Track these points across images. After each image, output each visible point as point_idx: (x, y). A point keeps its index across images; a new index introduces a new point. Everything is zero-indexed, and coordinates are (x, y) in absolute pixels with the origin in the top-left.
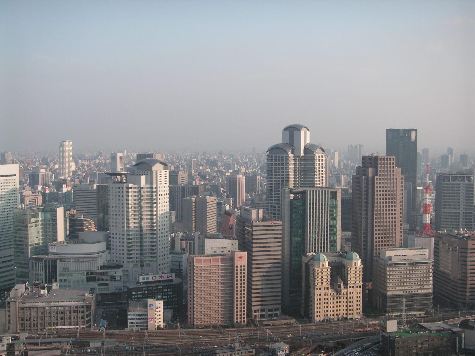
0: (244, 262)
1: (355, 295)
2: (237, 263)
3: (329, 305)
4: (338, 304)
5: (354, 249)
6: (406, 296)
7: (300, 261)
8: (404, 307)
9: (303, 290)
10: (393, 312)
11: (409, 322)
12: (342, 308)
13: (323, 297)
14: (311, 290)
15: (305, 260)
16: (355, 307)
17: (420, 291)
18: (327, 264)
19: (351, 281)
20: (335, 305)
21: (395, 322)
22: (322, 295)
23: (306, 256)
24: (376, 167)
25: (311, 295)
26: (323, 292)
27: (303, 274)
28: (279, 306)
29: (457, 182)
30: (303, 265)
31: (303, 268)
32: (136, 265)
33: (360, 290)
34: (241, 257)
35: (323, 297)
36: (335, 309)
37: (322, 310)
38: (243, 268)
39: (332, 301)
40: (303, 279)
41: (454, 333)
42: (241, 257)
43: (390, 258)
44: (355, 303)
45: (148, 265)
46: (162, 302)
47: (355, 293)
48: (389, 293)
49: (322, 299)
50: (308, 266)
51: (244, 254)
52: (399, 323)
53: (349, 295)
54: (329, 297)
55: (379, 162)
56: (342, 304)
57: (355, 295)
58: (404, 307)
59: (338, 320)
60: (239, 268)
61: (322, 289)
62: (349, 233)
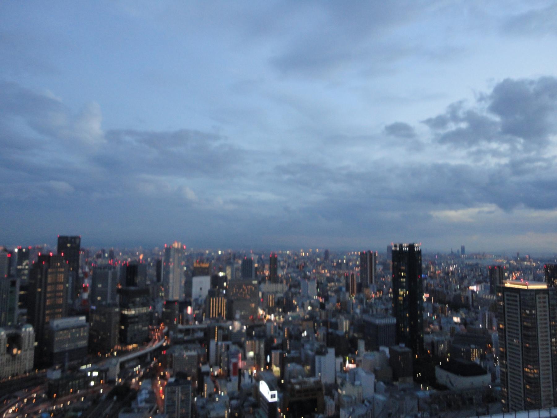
1: (28, 357)
18: (5, 337)
29: (106, 270)
33: (33, 352)
43: (57, 326)
52: (63, 372)
53: (23, 358)
57: (28, 357)
62: (25, 311)
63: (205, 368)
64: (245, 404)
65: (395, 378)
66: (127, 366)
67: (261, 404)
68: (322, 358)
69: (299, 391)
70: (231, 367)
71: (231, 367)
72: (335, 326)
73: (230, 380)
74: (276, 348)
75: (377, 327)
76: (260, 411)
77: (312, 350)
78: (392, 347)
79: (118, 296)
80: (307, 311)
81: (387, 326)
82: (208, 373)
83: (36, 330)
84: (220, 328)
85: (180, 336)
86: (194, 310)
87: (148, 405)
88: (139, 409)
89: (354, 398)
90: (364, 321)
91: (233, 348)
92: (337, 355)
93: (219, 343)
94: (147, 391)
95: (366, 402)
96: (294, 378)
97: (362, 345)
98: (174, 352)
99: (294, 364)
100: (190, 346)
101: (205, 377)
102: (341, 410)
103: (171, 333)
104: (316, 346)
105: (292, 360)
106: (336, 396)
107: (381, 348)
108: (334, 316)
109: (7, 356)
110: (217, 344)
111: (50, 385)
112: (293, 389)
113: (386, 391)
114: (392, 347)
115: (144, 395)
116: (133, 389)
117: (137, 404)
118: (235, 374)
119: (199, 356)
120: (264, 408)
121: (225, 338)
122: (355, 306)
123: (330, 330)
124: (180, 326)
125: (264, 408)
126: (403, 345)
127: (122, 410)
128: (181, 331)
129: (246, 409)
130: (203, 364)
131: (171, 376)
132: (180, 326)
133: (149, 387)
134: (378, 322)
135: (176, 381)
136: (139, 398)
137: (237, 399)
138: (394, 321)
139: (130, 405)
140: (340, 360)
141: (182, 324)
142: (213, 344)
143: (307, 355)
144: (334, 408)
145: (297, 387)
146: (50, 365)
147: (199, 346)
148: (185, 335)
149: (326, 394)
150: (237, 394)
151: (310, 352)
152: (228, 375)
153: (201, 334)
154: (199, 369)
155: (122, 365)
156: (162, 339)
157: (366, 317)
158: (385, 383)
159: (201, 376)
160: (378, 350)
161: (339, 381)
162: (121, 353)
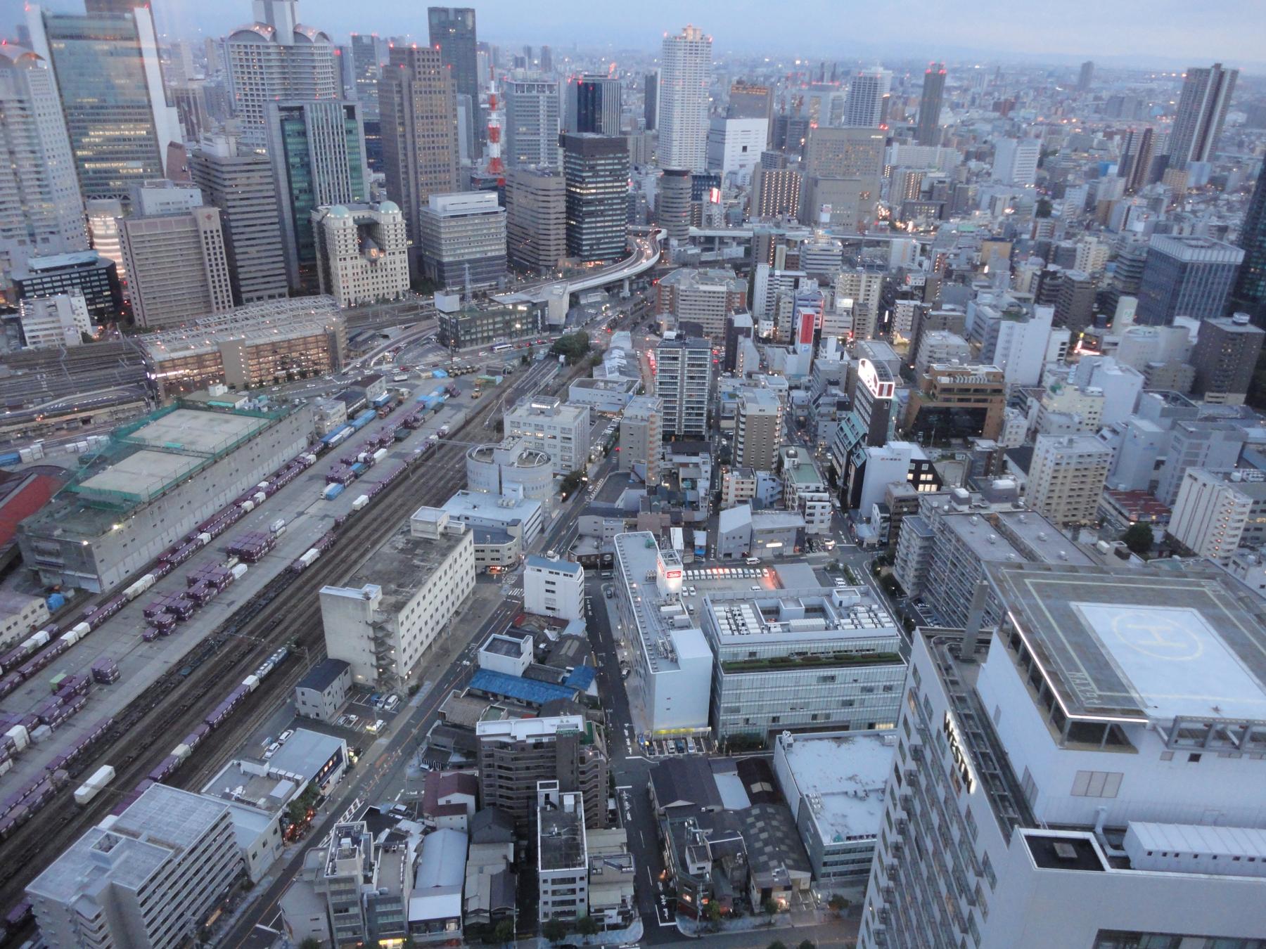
0: (216, 224)
1: (398, 265)
2: (204, 225)
3: (361, 282)
4: (375, 280)
5: (391, 197)
6: (469, 261)
7: (309, 221)
8: (467, 277)
9: (319, 263)
10: (454, 284)
11: (475, 296)
12: (380, 286)
13: (350, 272)
14: (332, 263)
15: (316, 217)
16: (400, 283)
17: (489, 254)
18: (350, 223)
19: (390, 245)
20: (370, 281)
21: (457, 297)
22: (349, 268)
23: (317, 211)
24: (412, 66)
25: (332, 270)
26: (349, 263)
27: (316, 239)
28: (286, 290)
29: (534, 93)
30: (314, 225)
31: (315, 230)
32: (22, 243)
33: (405, 256)
34: (209, 217)
35: (350, 272)
36: (371, 287)
37: (352, 290)
38: (215, 234)
39: (365, 276)
40: (317, 245)
41: (534, 304)
42: (209, 217)
44: (399, 278)
45: (45, 240)
46: (83, 299)
47: (398, 262)
48: (446, 260)
49: (350, 275)
50: (320, 223)
51: (215, 211)
52: (462, 299)
53: (389, 267)
54: (359, 270)
55: (416, 56)
56: (380, 279)
57: (398, 265)
58: (467, 277)
59: (377, 301)
60: (209, 235)
61: (348, 259)
62: (381, 176)
63: (742, 321)
64: (820, 401)
65: (1197, 390)
66: (583, 302)
67: (857, 402)
68: (1018, 326)
69: (947, 390)
70: (799, 325)
71: (799, 325)
72: (1068, 258)
73: (795, 352)
74: (905, 296)
75: (1183, 267)
76: (854, 415)
77: (994, 307)
78: (1212, 321)
79: (561, 151)
80: (1001, 219)
81: (1212, 268)
82: (746, 332)
83: (408, 217)
84: (783, 239)
85: (693, 250)
86: (725, 197)
87: (625, 379)
88: (606, 382)
89: (1077, 419)
90: (1151, 252)
91: (808, 286)
92: (1056, 324)
93: (778, 273)
94: (623, 354)
95: (1105, 432)
96: (939, 360)
97: (1127, 307)
98: (678, 281)
99: (945, 333)
100: (711, 272)
101: (741, 338)
102: (1039, 437)
103: (674, 242)
104: (1009, 298)
105: (944, 324)
106: (1033, 412)
107: (1179, 320)
108: (1069, 236)
109: (362, 262)
110: (771, 275)
111: (441, 319)
112: (932, 385)
113: (1165, 413)
114: (1212, 321)
115: (614, 360)
116: (595, 348)
117: (604, 375)
118: (805, 340)
119: (730, 294)
120: (862, 411)
121: (791, 263)
122: (1133, 214)
123: (1052, 267)
124: (693, 230)
125: (862, 411)
126: (1245, 318)
127: (577, 380)
128: (694, 240)
129: (823, 410)
130: (737, 312)
131: (670, 329)
132: (693, 230)
133: (627, 345)
134: (1187, 255)
135: (679, 337)
136: (608, 364)
137: (807, 389)
138: (1238, 256)
139: (591, 376)
140: (1064, 335)
141: (699, 225)
142: (762, 271)
143: (979, 318)
144: (1023, 431)
145: (945, 380)
146: (439, 285)
147: (733, 273)
148: (705, 250)
149: (1013, 405)
150: (805, 380)
151: (990, 312)
152: (792, 343)
153: (737, 252)
154: (730, 322)
155: (574, 297)
156: (655, 254)
157: (1160, 243)
158: (1165, 396)
159: (732, 335)
160: (1169, 322)
161: (1049, 380)
162: (570, 275)
